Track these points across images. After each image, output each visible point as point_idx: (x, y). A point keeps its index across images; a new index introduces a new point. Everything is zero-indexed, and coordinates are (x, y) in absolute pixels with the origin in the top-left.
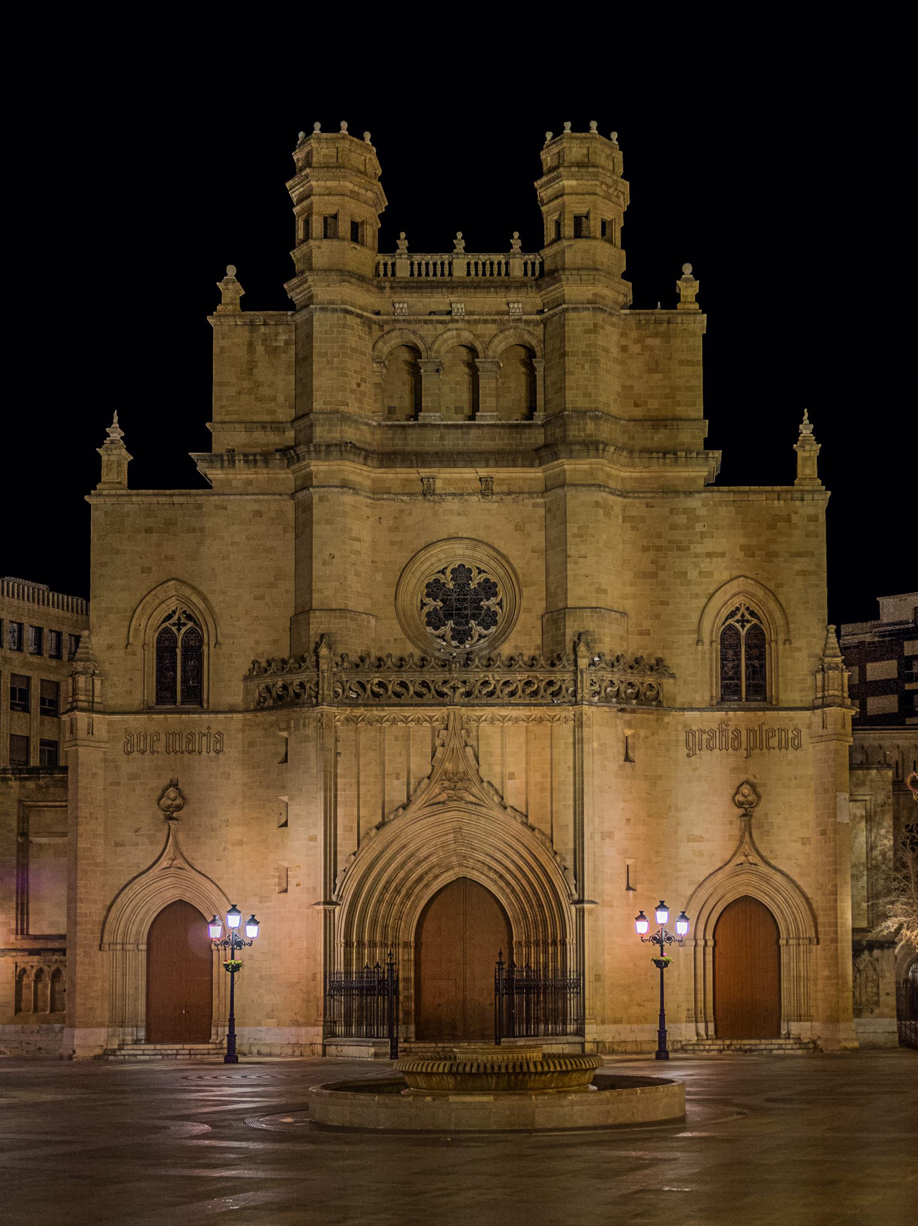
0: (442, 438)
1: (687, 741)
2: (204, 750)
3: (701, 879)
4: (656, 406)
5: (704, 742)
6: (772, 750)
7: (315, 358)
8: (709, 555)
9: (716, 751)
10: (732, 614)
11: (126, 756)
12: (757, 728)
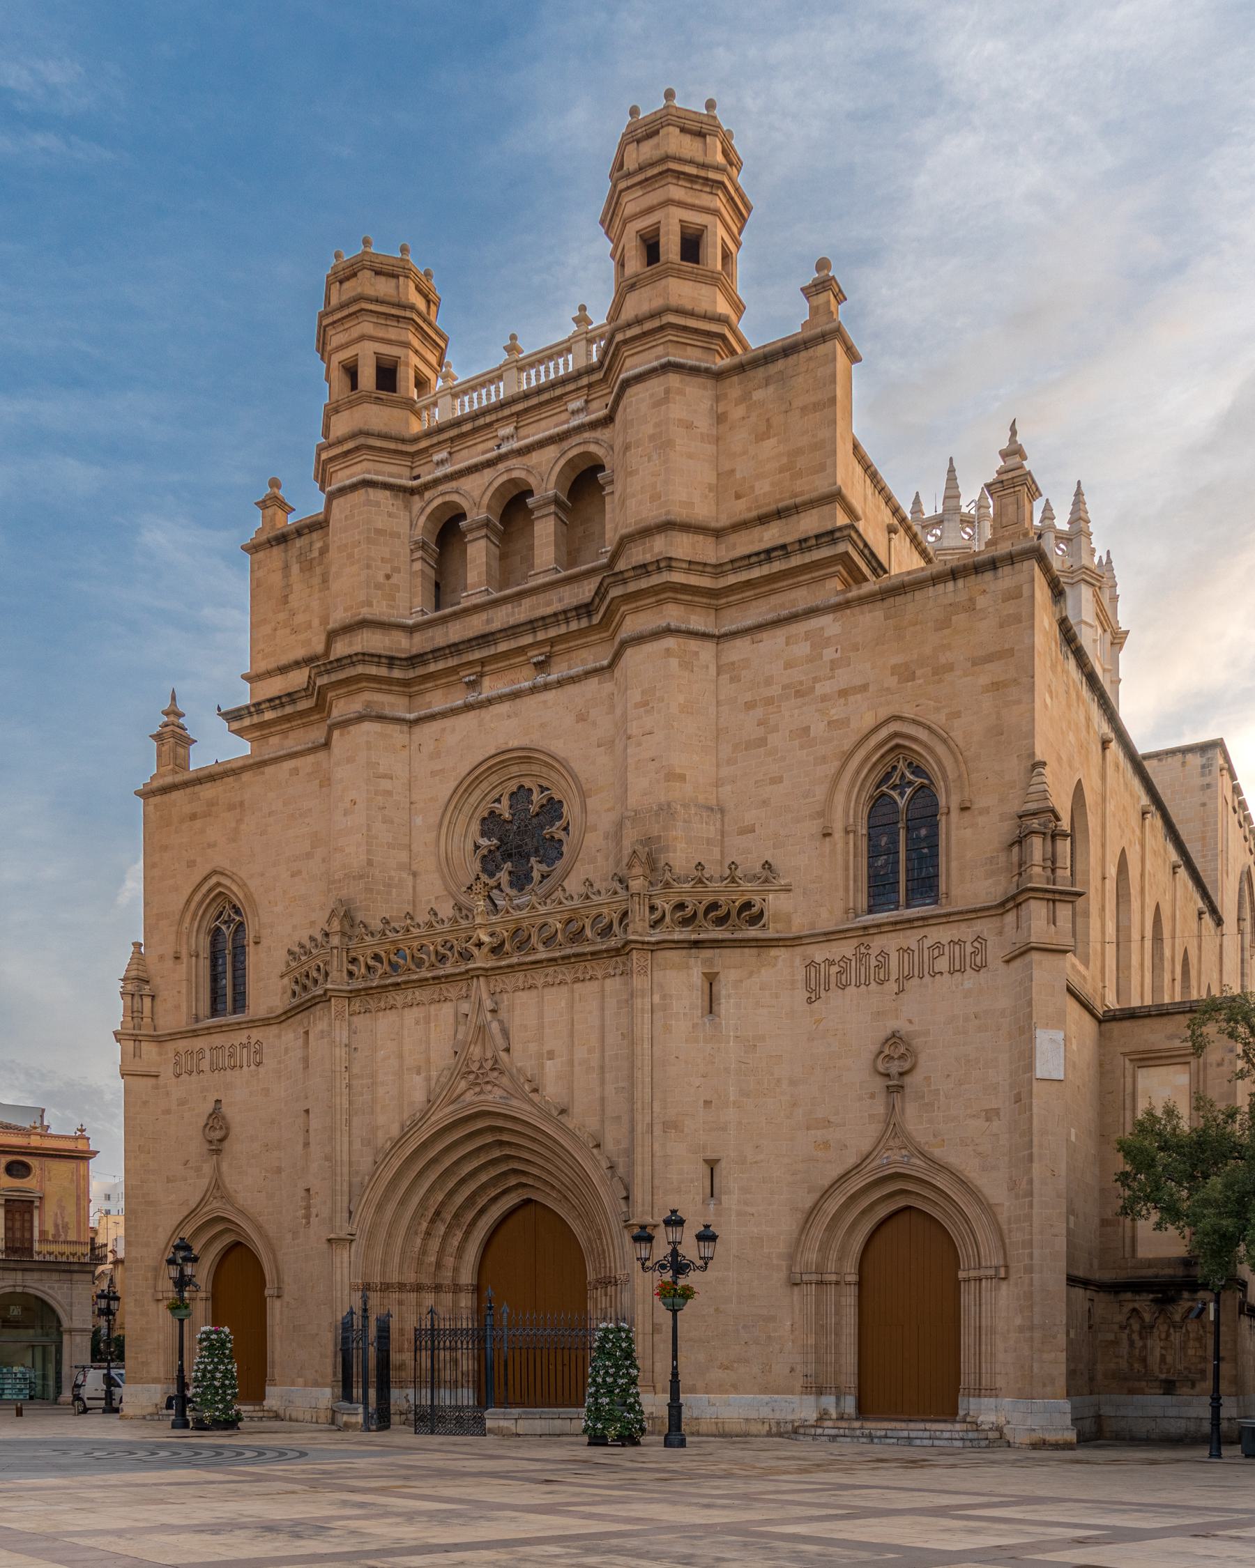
1: (807, 981)
5: (833, 979)
6: (938, 976)
9: (852, 990)
12: (914, 946)
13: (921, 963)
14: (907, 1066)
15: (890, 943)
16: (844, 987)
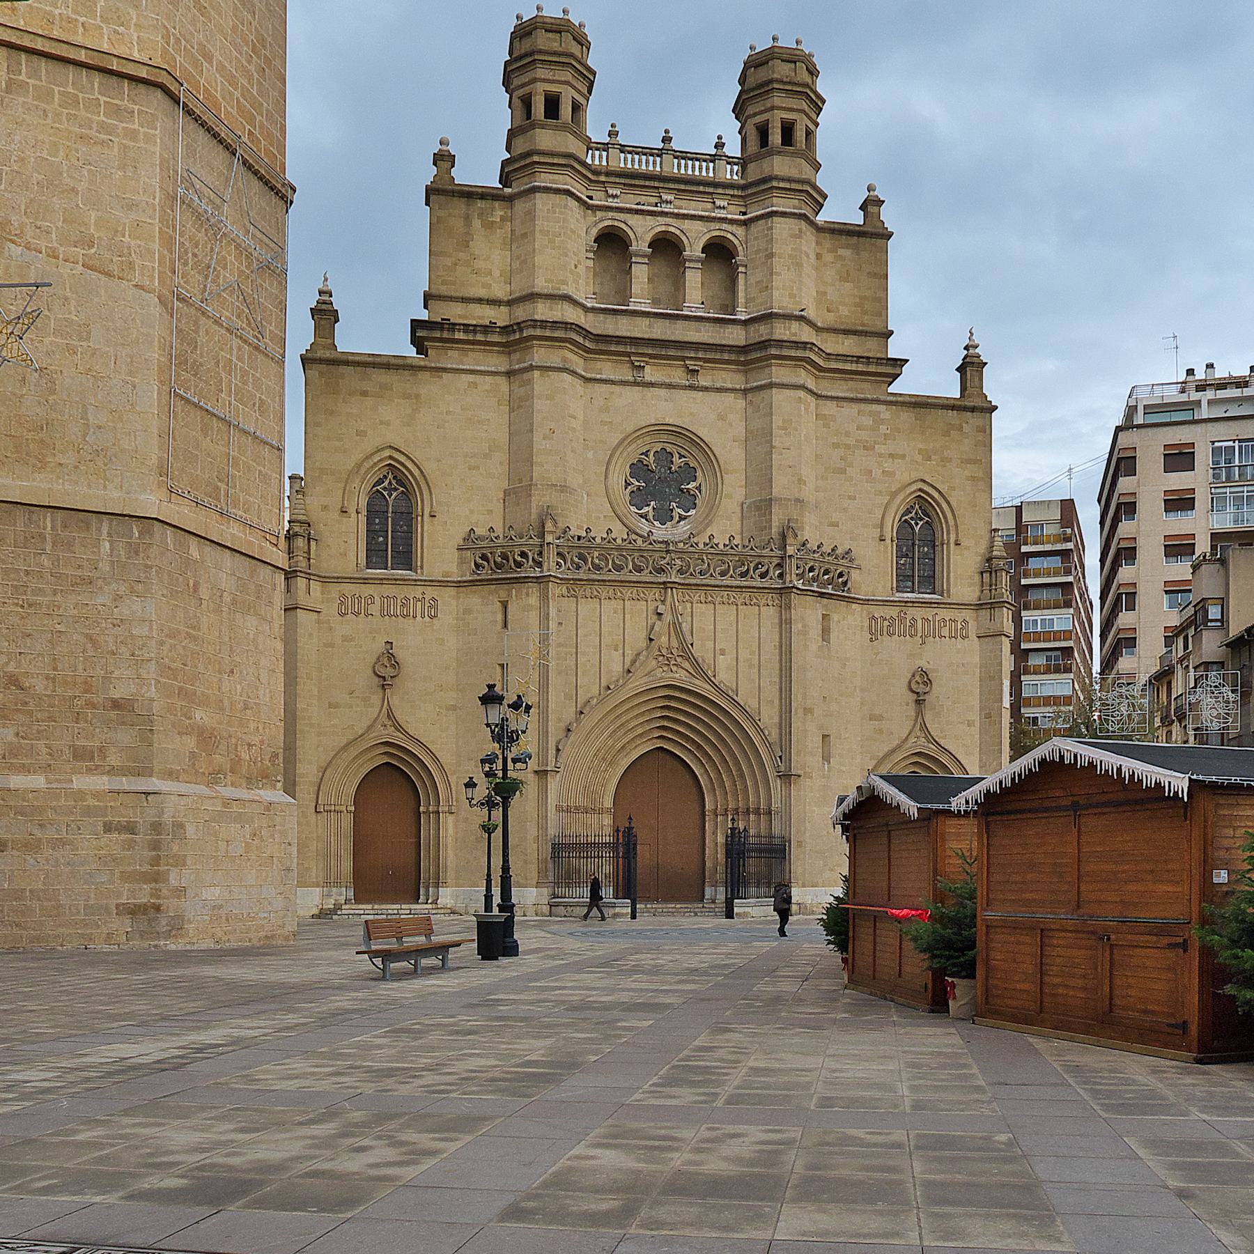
0: (650, 326)
1: (870, 626)
2: (419, 615)
3: (881, 755)
4: (847, 313)
5: (885, 629)
7: (537, 234)
8: (891, 456)
10: (908, 512)
11: (341, 618)
12: (931, 619)
13: (934, 629)
14: (928, 689)
15: (917, 613)
16: (890, 635)
